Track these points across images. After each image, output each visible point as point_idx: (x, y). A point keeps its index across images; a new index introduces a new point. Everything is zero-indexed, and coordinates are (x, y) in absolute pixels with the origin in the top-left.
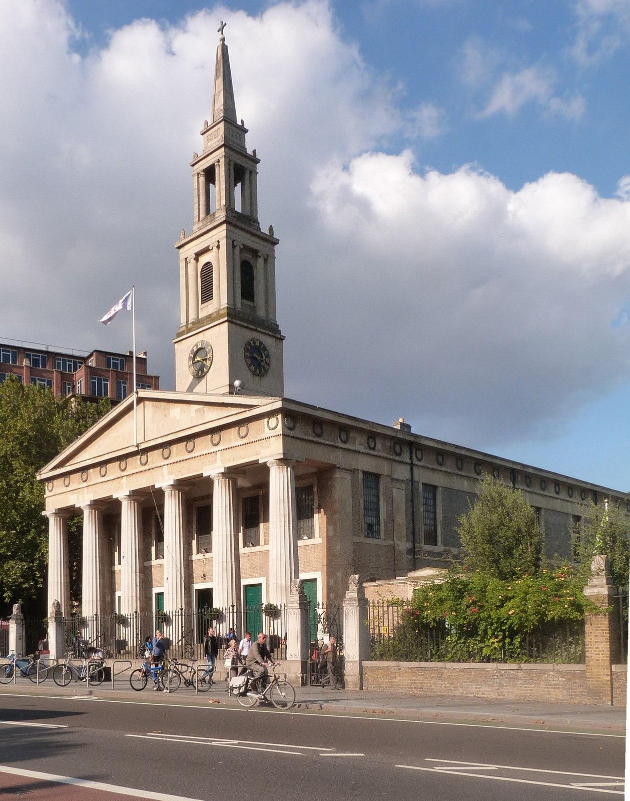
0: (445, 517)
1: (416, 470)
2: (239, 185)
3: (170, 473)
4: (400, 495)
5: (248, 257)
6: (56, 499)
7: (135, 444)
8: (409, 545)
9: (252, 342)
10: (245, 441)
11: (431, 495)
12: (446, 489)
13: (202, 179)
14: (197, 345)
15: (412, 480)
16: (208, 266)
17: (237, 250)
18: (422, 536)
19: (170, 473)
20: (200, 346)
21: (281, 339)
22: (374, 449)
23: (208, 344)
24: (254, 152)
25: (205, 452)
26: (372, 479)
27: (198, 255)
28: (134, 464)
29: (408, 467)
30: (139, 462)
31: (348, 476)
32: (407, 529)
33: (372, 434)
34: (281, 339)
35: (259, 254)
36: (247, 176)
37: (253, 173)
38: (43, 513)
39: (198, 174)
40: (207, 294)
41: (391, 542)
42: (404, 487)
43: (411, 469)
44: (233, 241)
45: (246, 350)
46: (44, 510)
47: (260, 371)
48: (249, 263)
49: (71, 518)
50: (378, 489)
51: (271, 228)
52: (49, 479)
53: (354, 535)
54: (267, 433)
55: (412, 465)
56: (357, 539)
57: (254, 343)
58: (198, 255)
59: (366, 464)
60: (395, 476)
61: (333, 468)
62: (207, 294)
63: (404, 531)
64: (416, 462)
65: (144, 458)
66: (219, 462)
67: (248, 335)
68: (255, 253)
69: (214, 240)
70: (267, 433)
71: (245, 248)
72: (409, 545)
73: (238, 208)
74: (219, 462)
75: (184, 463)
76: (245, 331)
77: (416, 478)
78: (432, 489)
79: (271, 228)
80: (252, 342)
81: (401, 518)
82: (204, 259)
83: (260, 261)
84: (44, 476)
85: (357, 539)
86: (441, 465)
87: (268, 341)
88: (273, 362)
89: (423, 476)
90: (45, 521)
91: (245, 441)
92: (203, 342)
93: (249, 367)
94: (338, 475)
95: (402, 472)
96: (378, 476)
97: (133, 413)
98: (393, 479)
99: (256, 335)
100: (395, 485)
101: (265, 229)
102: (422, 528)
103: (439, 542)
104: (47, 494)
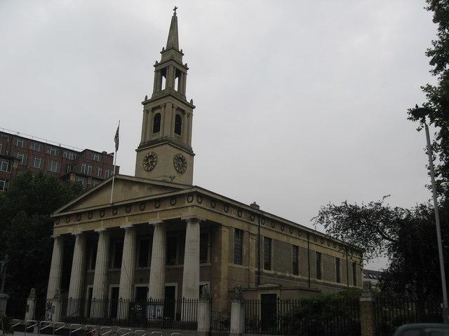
0: (275, 256)
1: (261, 229)
3: (129, 221)
4: (253, 242)
8: (257, 269)
10: (174, 207)
11: (268, 244)
12: (276, 240)
16: (159, 115)
18: (263, 265)
19: (129, 221)
21: (194, 155)
23: (155, 154)
24: (186, 64)
26: (239, 232)
28: (109, 215)
31: (227, 230)
34: (194, 155)
36: (182, 75)
37: (185, 74)
40: (156, 128)
49: (68, 242)
52: (58, 218)
53: (229, 262)
54: (187, 204)
56: (230, 264)
58: (154, 109)
59: (237, 225)
61: (220, 225)
62: (156, 128)
63: (254, 261)
66: (158, 217)
67: (178, 152)
68: (183, 111)
70: (187, 204)
71: (178, 109)
72: (257, 269)
73: (176, 89)
74: (158, 217)
76: (175, 150)
78: (269, 240)
81: (253, 255)
82: (157, 112)
83: (186, 115)
84: (55, 216)
85: (230, 264)
86: (273, 227)
87: (186, 156)
89: (264, 233)
91: (174, 207)
93: (176, 168)
94: (223, 229)
95: (254, 230)
96: (242, 231)
99: (181, 152)
101: (188, 101)
102: (263, 261)
103: (272, 268)
104: (55, 225)
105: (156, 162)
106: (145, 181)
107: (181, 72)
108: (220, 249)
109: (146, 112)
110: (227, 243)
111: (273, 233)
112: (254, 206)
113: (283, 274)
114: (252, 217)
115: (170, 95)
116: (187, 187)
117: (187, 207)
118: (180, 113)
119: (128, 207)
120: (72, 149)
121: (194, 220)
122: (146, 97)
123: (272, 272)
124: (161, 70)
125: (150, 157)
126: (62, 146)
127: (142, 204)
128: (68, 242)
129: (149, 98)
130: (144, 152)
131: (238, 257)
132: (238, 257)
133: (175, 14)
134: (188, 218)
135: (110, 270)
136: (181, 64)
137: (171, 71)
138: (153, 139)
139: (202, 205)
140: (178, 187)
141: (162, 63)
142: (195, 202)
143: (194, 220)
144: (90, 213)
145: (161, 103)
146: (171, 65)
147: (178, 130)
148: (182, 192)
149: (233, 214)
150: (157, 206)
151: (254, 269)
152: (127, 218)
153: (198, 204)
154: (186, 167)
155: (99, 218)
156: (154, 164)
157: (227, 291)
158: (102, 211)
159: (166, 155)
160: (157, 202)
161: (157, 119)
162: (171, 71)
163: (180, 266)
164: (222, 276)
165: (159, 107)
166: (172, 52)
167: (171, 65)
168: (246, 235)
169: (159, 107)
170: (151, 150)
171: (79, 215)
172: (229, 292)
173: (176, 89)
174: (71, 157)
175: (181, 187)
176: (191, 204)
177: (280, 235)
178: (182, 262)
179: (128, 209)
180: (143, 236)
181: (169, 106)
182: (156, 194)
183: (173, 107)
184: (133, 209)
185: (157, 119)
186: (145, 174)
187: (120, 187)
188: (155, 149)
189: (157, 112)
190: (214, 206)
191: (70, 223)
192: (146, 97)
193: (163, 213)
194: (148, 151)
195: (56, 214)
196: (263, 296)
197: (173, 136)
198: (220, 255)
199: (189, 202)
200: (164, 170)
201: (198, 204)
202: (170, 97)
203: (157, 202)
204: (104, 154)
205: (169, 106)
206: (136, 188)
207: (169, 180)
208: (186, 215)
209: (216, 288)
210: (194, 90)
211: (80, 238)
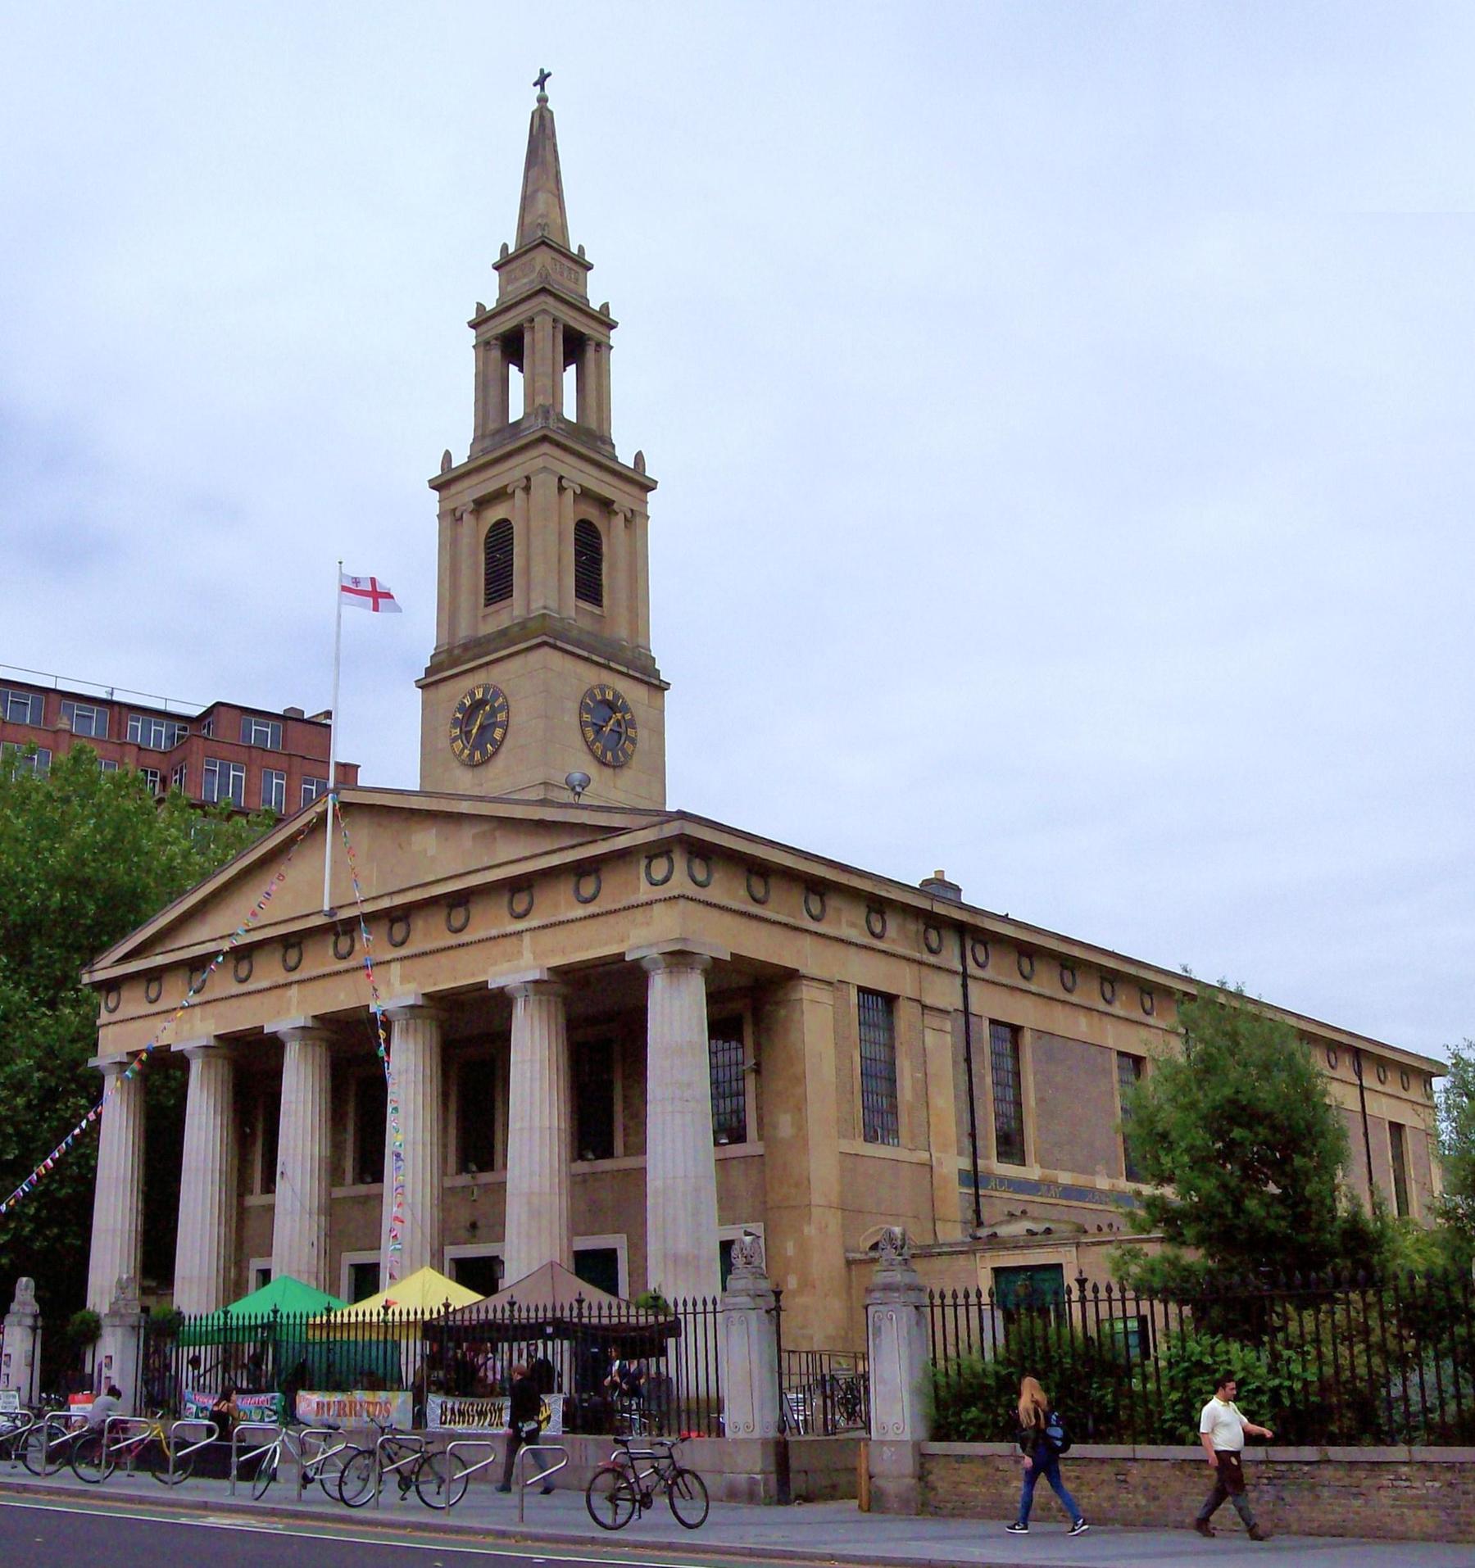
2: (572, 369)
3: (404, 979)
4: (941, 1044)
5: (592, 514)
6: (124, 1033)
7: (326, 908)
9: (597, 691)
10: (592, 909)
13: (496, 354)
14: (472, 694)
15: (966, 1012)
17: (569, 494)
19: (404, 979)
20: (479, 696)
21: (661, 687)
22: (879, 937)
23: (497, 693)
25: (494, 932)
26: (880, 1004)
27: (482, 504)
28: (319, 959)
29: (958, 981)
30: (331, 952)
32: (959, 1123)
33: (877, 901)
34: (661, 687)
35: (615, 507)
38: (93, 1062)
39: (487, 343)
40: (498, 584)
41: (925, 1156)
42: (948, 1027)
43: (965, 986)
44: (561, 478)
45: (583, 707)
46: (96, 1054)
47: (615, 756)
48: (591, 524)
49: (161, 1078)
50: (891, 1029)
51: (639, 457)
52: (111, 986)
53: (842, 1135)
54: (645, 892)
55: (965, 976)
56: (846, 1146)
57: (603, 694)
58: (482, 504)
60: (928, 1001)
62: (498, 584)
64: (972, 968)
65: (344, 944)
66: (528, 956)
67: (590, 676)
68: (606, 505)
69: (518, 474)
70: (645, 892)
71: (585, 494)
73: (570, 412)
74: (528, 956)
75: (443, 958)
76: (582, 668)
77: (974, 1008)
79: (639, 457)
80: (597, 691)
83: (619, 521)
84: (100, 976)
85: (846, 1146)
88: (642, 734)
89: (988, 1004)
90: (92, 1089)
91: (592, 909)
94: (807, 993)
95: (945, 993)
96: (890, 1000)
98: (924, 1007)
99: (606, 677)
100: (932, 1020)
101: (626, 458)
105: (505, 726)
106: (465, 807)
107: (583, 342)
108: (800, 1079)
109: (450, 517)
110: (830, 1052)
111: (1028, 1002)
112: (939, 887)
113: (1081, 1180)
114: (933, 936)
115: (544, 439)
118: (592, 514)
120: (159, 705)
121: (679, 959)
122: (447, 456)
123: (1032, 1172)
124: (503, 343)
125: (479, 705)
126: (118, 697)
128: (161, 1078)
129: (460, 459)
130: (444, 690)
131: (880, 1113)
132: (880, 1113)
134: (654, 953)
135: (339, 1192)
136: (583, 309)
137: (543, 343)
138: (488, 628)
139: (714, 893)
140: (602, 820)
141: (503, 309)
142: (680, 882)
143: (679, 959)
145: (509, 474)
146: (543, 318)
147: (589, 587)
148: (622, 842)
149: (848, 922)
151: (953, 1163)
152: (396, 968)
153: (691, 890)
154: (633, 741)
155: (282, 977)
156: (498, 733)
157: (842, 1263)
159: (541, 693)
161: (500, 541)
162: (543, 343)
163: (631, 1162)
164: (816, 1198)
165: (501, 495)
166: (543, 257)
167: (543, 318)
168: (905, 1014)
169: (501, 495)
170: (481, 677)
172: (849, 1263)
173: (570, 412)
174: (158, 736)
175: (617, 821)
177: (1059, 1012)
178: (639, 1148)
179: (399, 931)
180: (470, 1042)
181: (544, 487)
182: (514, 856)
183: (561, 489)
185: (500, 541)
186: (464, 780)
187: (362, 834)
190: (760, 893)
192: (447, 456)
193: (548, 939)
194: (468, 683)
195: (105, 968)
196: (998, 1272)
197: (571, 606)
198: (800, 1108)
200: (544, 755)
201: (691, 890)
202: (546, 448)
204: (292, 718)
205: (544, 487)
207: (567, 797)
208: (638, 937)
209: (790, 1249)
210: (643, 414)
211: (207, 1065)
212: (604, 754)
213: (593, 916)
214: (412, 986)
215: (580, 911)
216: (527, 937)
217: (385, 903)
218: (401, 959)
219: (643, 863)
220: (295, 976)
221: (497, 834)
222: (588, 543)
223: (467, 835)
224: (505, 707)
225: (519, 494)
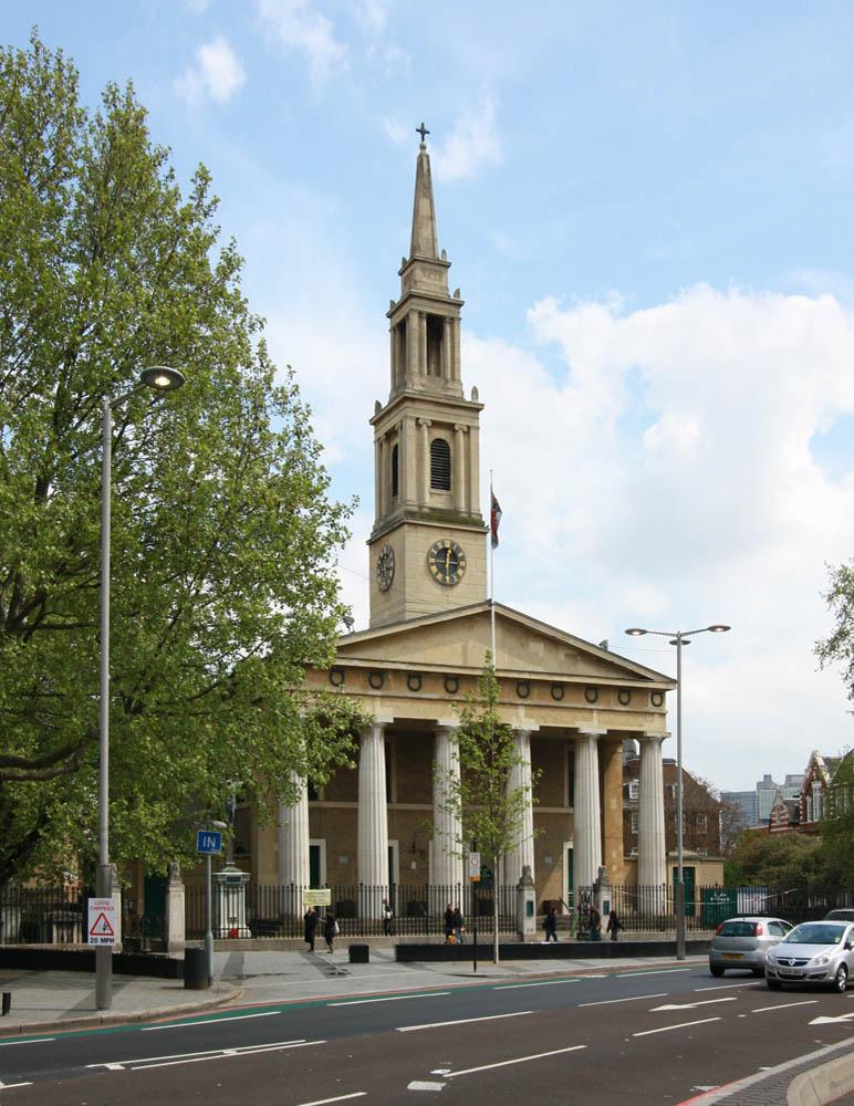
3: (527, 716)
25: (580, 706)
54: (650, 708)
57: (444, 545)
58: (436, 424)
66: (595, 722)
70: (650, 708)
75: (549, 712)
92: (453, 544)
97: (479, 630)
105: (463, 568)
116: (660, 679)
117: (653, 713)
119: (523, 687)
127: (558, 689)
133: (423, 147)
140: (642, 673)
144: (415, 678)
150: (592, 698)
158: (453, 682)
160: (593, 692)
163: (571, 811)
165: (450, 427)
171: (376, 677)
176: (653, 709)
184: (535, 691)
188: (456, 534)
189: (442, 434)
191: (346, 689)
193: (606, 716)
199: (654, 704)
203: (593, 692)
206: (537, 647)
212: (444, 579)
213: (628, 712)
214: (532, 721)
215: (623, 708)
216: (595, 714)
217: (527, 676)
218: (526, 705)
219: (650, 695)
220: (458, 698)
221: (579, 658)
222: (441, 452)
223: (561, 655)
224: (463, 558)
225: (461, 437)
